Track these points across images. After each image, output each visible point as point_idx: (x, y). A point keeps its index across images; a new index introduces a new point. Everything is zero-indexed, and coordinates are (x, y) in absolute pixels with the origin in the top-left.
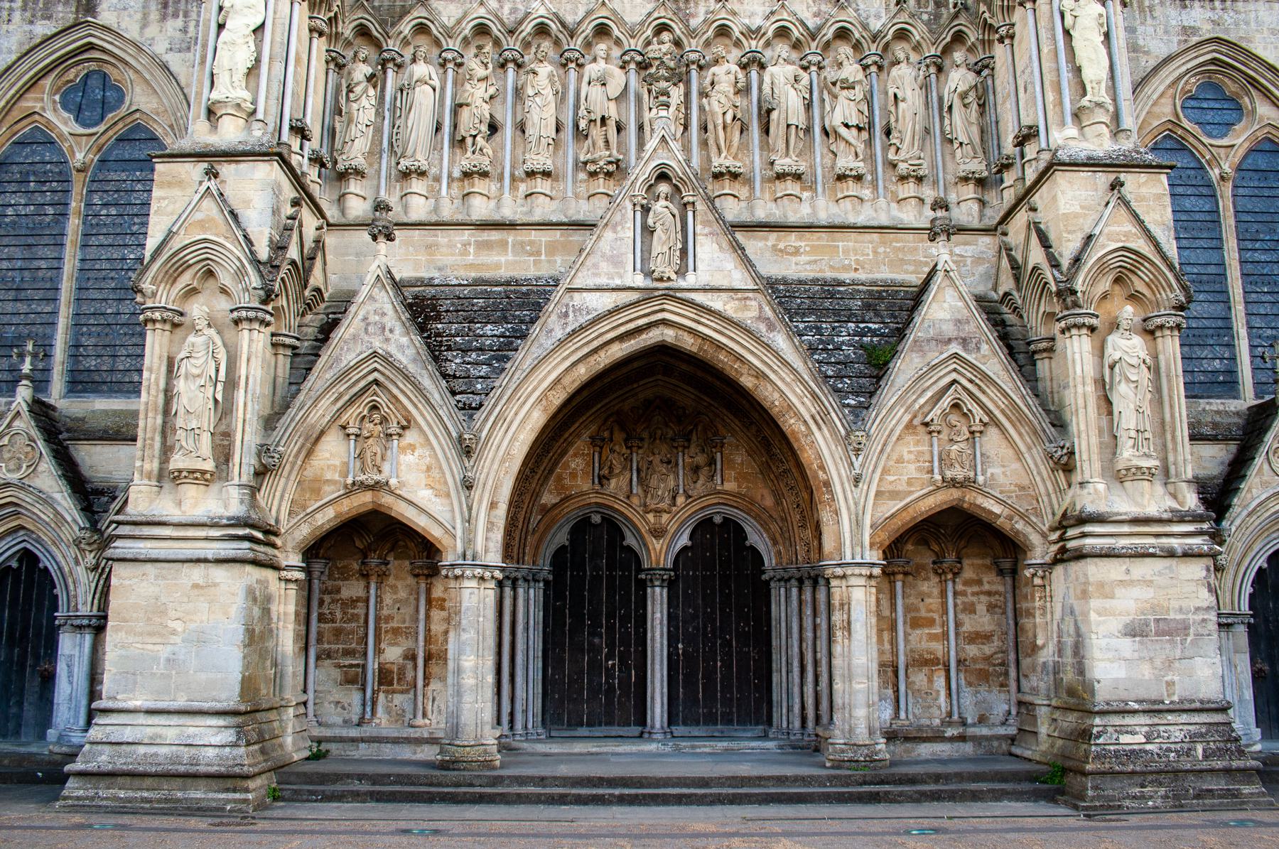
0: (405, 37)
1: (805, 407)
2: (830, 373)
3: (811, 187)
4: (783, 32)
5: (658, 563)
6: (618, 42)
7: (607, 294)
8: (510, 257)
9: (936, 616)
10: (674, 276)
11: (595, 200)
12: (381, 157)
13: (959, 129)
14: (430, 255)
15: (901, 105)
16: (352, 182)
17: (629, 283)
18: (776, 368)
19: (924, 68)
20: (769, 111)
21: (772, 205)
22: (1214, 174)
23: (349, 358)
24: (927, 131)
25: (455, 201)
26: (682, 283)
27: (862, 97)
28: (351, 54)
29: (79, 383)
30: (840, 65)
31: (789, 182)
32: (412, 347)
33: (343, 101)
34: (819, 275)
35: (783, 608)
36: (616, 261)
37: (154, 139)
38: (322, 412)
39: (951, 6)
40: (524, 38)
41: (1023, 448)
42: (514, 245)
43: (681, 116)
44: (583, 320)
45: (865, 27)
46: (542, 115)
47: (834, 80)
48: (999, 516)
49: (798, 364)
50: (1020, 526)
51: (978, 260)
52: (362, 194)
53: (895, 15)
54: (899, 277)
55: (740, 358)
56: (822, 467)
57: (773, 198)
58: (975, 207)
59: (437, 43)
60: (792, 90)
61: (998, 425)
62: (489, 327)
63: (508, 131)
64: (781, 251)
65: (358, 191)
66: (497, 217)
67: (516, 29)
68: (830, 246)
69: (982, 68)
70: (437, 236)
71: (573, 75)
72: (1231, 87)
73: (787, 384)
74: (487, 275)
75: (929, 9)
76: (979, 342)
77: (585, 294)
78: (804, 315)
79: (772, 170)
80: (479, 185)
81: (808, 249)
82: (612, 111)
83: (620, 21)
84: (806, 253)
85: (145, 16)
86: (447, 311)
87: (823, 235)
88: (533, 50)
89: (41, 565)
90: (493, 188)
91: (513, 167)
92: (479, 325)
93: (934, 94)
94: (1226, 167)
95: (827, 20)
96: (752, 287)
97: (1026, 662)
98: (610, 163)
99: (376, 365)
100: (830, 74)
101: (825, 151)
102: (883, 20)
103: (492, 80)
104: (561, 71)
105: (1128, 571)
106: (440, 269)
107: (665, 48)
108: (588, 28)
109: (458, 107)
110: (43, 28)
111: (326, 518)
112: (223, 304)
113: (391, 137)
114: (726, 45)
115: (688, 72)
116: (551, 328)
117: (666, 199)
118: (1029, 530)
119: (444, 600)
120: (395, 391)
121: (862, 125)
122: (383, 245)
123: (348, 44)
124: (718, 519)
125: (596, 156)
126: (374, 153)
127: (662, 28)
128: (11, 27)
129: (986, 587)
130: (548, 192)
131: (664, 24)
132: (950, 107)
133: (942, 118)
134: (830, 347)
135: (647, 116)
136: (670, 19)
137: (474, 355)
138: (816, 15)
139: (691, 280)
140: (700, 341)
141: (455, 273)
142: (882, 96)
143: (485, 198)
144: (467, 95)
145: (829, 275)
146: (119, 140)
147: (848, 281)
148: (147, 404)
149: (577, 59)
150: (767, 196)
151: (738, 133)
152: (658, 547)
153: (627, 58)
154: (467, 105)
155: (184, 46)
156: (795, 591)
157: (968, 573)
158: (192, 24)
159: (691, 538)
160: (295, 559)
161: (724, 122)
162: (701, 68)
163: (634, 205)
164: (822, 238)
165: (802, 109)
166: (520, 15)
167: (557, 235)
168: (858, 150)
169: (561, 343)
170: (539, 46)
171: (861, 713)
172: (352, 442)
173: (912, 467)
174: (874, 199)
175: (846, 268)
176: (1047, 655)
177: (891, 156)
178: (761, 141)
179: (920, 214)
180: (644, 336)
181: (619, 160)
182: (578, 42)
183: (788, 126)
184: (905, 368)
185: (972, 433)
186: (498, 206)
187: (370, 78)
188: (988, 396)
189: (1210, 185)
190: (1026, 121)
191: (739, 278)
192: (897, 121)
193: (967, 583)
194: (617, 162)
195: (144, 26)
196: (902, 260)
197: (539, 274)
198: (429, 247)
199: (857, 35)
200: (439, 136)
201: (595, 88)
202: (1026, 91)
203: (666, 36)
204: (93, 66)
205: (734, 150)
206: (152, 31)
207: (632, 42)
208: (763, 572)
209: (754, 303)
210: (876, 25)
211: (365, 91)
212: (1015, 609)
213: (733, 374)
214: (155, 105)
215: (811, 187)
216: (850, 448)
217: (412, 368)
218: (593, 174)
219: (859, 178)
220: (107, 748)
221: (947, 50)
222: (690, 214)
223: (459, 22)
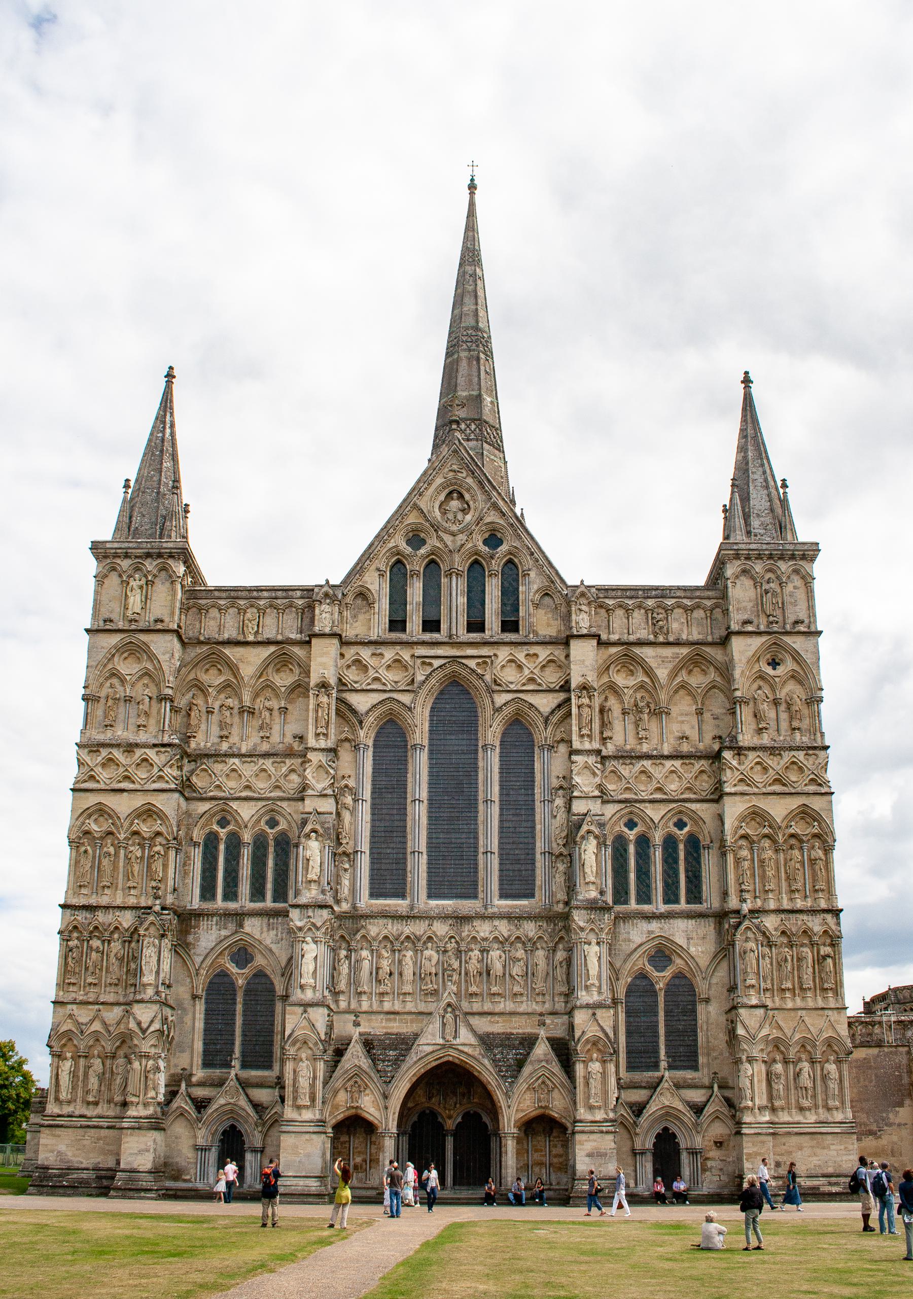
21: (490, 1004)
22: (657, 987)
24: (548, 974)
26: (455, 1042)
29: (244, 1066)
36: (433, 1035)
37: (266, 976)
38: (339, 1084)
45: (527, 936)
46: (408, 971)
49: (492, 1070)
50: (564, 1121)
51: (563, 1024)
66: (392, 1010)
69: (570, 950)
72: (667, 953)
74: (389, 1031)
83: (436, 936)
94: (661, 986)
108: (424, 938)
109: (378, 969)
110: (224, 933)
111: (340, 1117)
112: (310, 1052)
116: (413, 1057)
126: (349, 984)
139: (458, 1041)
145: (509, 1030)
146: (254, 975)
160: (330, 1130)
169: (416, 1062)
182: (420, 944)
184: (527, 1070)
187: (346, 957)
189: (655, 992)
191: (473, 1040)
195: (262, 933)
203: (453, 940)
206: (265, 935)
210: (531, 934)
217: (368, 1070)
218: (427, 994)
219: (522, 994)
223: (378, 934)
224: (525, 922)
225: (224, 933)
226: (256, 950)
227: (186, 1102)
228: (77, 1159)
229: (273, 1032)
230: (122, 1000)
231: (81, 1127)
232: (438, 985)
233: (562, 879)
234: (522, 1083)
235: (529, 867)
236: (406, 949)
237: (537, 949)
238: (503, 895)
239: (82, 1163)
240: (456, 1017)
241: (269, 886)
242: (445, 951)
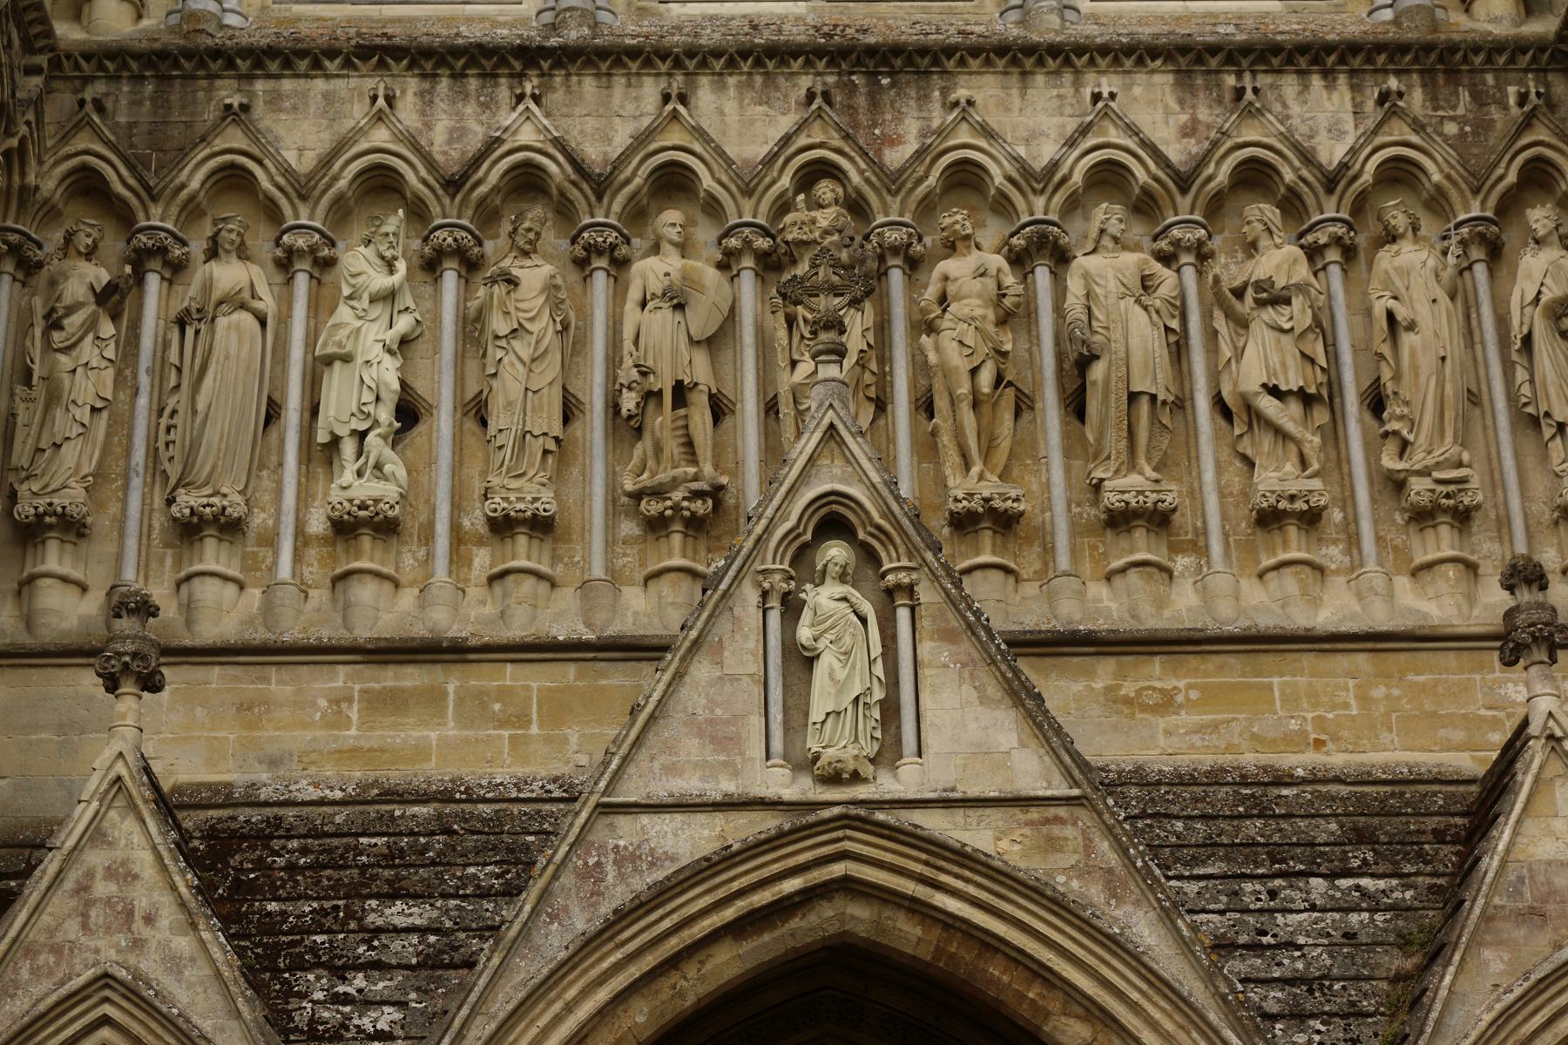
0: (192, 198)
2: (1272, 1007)
3: (1194, 543)
4: (1108, 177)
6: (712, 207)
7: (701, 818)
8: (451, 731)
10: (867, 770)
11: (665, 586)
12: (126, 487)
13: (1552, 391)
14: (252, 725)
15: (1407, 340)
16: (53, 547)
17: (759, 791)
18: (1135, 996)
19: (1455, 250)
20: (1085, 362)
21: (1098, 590)
23: (37, 990)
24: (1473, 399)
25: (312, 593)
26: (886, 785)
27: (1308, 321)
28: (58, 236)
30: (1252, 248)
31: (1140, 535)
32: (201, 962)
33: (37, 353)
34: (1226, 760)
36: (723, 738)
39: (1512, 101)
40: (482, 201)
42: (460, 701)
43: (868, 378)
44: (643, 881)
45: (1308, 157)
47: (1237, 283)
52: (77, 574)
53: (1379, 125)
54: (1429, 759)
57: (1103, 571)
59: (272, 213)
60: (1138, 309)
63: (443, 422)
64: (1128, 701)
65: (66, 569)
66: (420, 631)
67: (465, 176)
68: (1250, 686)
70: (266, 680)
71: (600, 279)
74: (394, 776)
75: (1460, 111)
77: (645, 819)
78: (1195, 861)
79: (1096, 502)
80: (369, 556)
81: (1194, 695)
82: (700, 370)
86: (292, 868)
87: (1232, 659)
88: (506, 227)
90: (408, 560)
91: (457, 507)
92: (374, 903)
93: (1486, 310)
95: (1215, 144)
96: (1062, 789)
98: (697, 495)
99: (107, 1009)
100: (1230, 269)
101: (1226, 453)
102: (1350, 141)
103: (407, 300)
104: (574, 276)
106: (273, 763)
107: (825, 218)
108: (638, 175)
109: (318, 367)
113: (152, 440)
114: (972, 209)
115: (883, 274)
117: (842, 578)
121: (1312, 390)
122: (129, 704)
123: (51, 213)
125: (663, 476)
127: (814, 173)
130: (544, 568)
131: (821, 161)
132: (1527, 341)
134: (1266, 940)
135: (786, 381)
136: (839, 151)
137: (360, 981)
138: (1189, 131)
140: (936, 932)
141: (313, 770)
142: (1358, 319)
143: (388, 586)
144: (342, 334)
145: (1250, 759)
147: (1300, 772)
149: (613, 247)
150: (1087, 567)
151: (1007, 417)
153: (733, 242)
154: (347, 359)
161: (975, 391)
162: (914, 264)
163: (765, 595)
164: (1230, 670)
165: (1162, 356)
166: (474, 143)
167: (567, 674)
168: (1307, 450)
169: (590, 944)
170: (520, 217)
174: (1352, 569)
175: (1295, 742)
177: (1389, 462)
178: (1066, 436)
179: (1471, 600)
180: (795, 923)
181: (719, 488)
183: (1133, 397)
186: (423, 603)
187: (112, 298)
192: (1397, 378)
194: (717, 492)
196: (1434, 714)
197: (521, 771)
198: (245, 707)
199: (1289, 176)
200: (274, 435)
201: (659, 314)
203: (826, 189)
205: (1000, 457)
207: (747, 205)
209: (1069, 832)
210: (1332, 153)
211: (91, 325)
213: (1025, 1011)
215: (1194, 543)
218: (656, 526)
219: (1311, 519)
221: (1510, 205)
222: (903, 615)
223: (326, 162)
224: (1289, 85)
232: (737, 471)
237: (1392, 237)
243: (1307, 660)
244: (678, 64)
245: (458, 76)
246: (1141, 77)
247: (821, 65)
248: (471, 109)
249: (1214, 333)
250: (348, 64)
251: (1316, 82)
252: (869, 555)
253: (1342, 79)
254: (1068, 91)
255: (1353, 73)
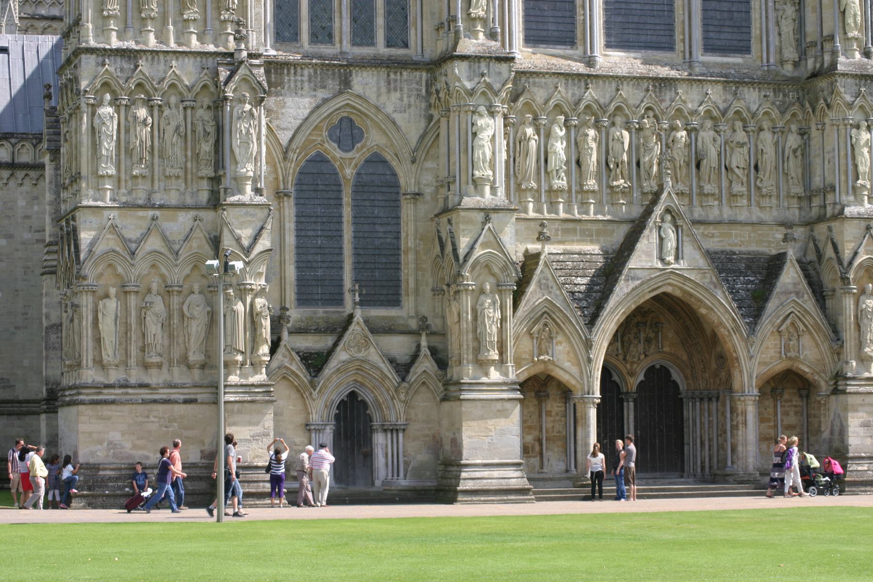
1: (729, 324)
5: (632, 390)
9: (771, 417)
15: (765, 156)
34: (723, 248)
35: (691, 412)
36: (649, 254)
37: (384, 162)
41: (820, 343)
42: (580, 231)
48: (807, 373)
50: (816, 378)
55: (700, 300)
56: (735, 351)
58: (797, 212)
61: (810, 333)
62: (579, 279)
64: (706, 235)
73: (722, 313)
76: (803, 294)
84: (717, 236)
85: (379, 89)
89: (359, 399)
97: (812, 439)
105: (863, 400)
108: (612, 107)
118: (820, 379)
119: (551, 412)
120: (554, 317)
124: (658, 366)
128: (304, 93)
129: (794, 403)
132: (788, 158)
133: (783, 162)
138: (725, 101)
145: (728, 248)
148: (467, 328)
152: (632, 381)
155: (403, 109)
156: (698, 404)
157: (786, 396)
158: (405, 96)
159: (645, 376)
164: (724, 229)
166: (577, 98)
171: (751, 460)
172: (535, 341)
173: (772, 351)
175: (736, 245)
176: (826, 435)
184: (771, 305)
185: (799, 336)
188: (806, 319)
190: (829, 180)
191: (702, 262)
192: (762, 163)
193: (786, 401)
199: (745, 115)
202: (829, 163)
203: (651, 114)
204: (345, 115)
206: (383, 98)
208: (680, 394)
209: (708, 275)
210: (754, 108)
212: (807, 414)
213: (695, 307)
214: (385, 142)
216: (749, 344)
220: (471, 481)
222: (680, 231)
224: (746, 90)
225: (322, 94)
226: (369, 122)
227: (292, 359)
228: (140, 452)
229: (399, 249)
230: (189, 201)
231: (144, 402)
233: (791, 28)
234: (767, 324)
235: (743, 7)
236: (585, 124)
238: (709, 48)
239: (147, 458)
240: (677, 227)
241: (380, 21)
242: (640, 129)
243: (739, 227)
244: (620, 79)
245: (573, 80)
246: (716, 86)
247: (650, 81)
248: (576, 88)
249: (725, 150)
250: (550, 76)
251: (751, 89)
252: (673, 217)
253: (757, 89)
254: (700, 89)
255: (759, 88)
